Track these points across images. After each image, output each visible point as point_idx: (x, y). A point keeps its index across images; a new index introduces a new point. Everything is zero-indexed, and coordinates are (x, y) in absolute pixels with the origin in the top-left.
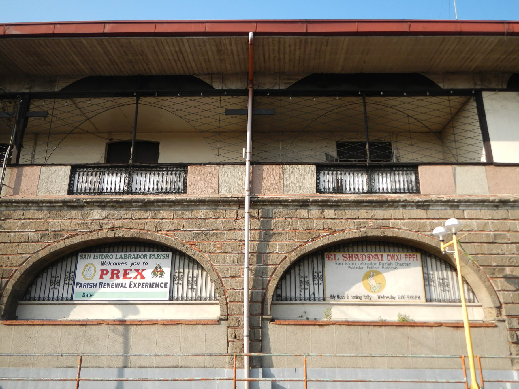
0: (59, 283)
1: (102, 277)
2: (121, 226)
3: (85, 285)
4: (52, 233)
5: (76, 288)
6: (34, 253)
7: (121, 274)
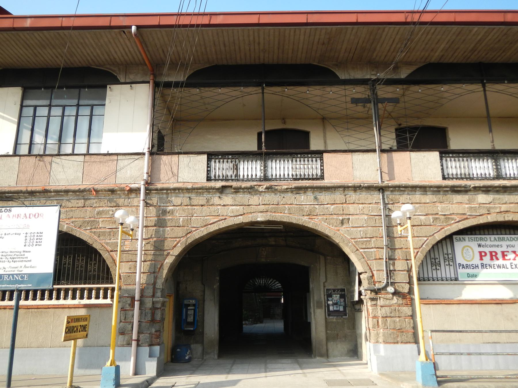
0: (440, 264)
1: (481, 259)
2: (509, 210)
3: (467, 266)
4: (443, 217)
5: (459, 268)
6: (430, 236)
7: (500, 256)
